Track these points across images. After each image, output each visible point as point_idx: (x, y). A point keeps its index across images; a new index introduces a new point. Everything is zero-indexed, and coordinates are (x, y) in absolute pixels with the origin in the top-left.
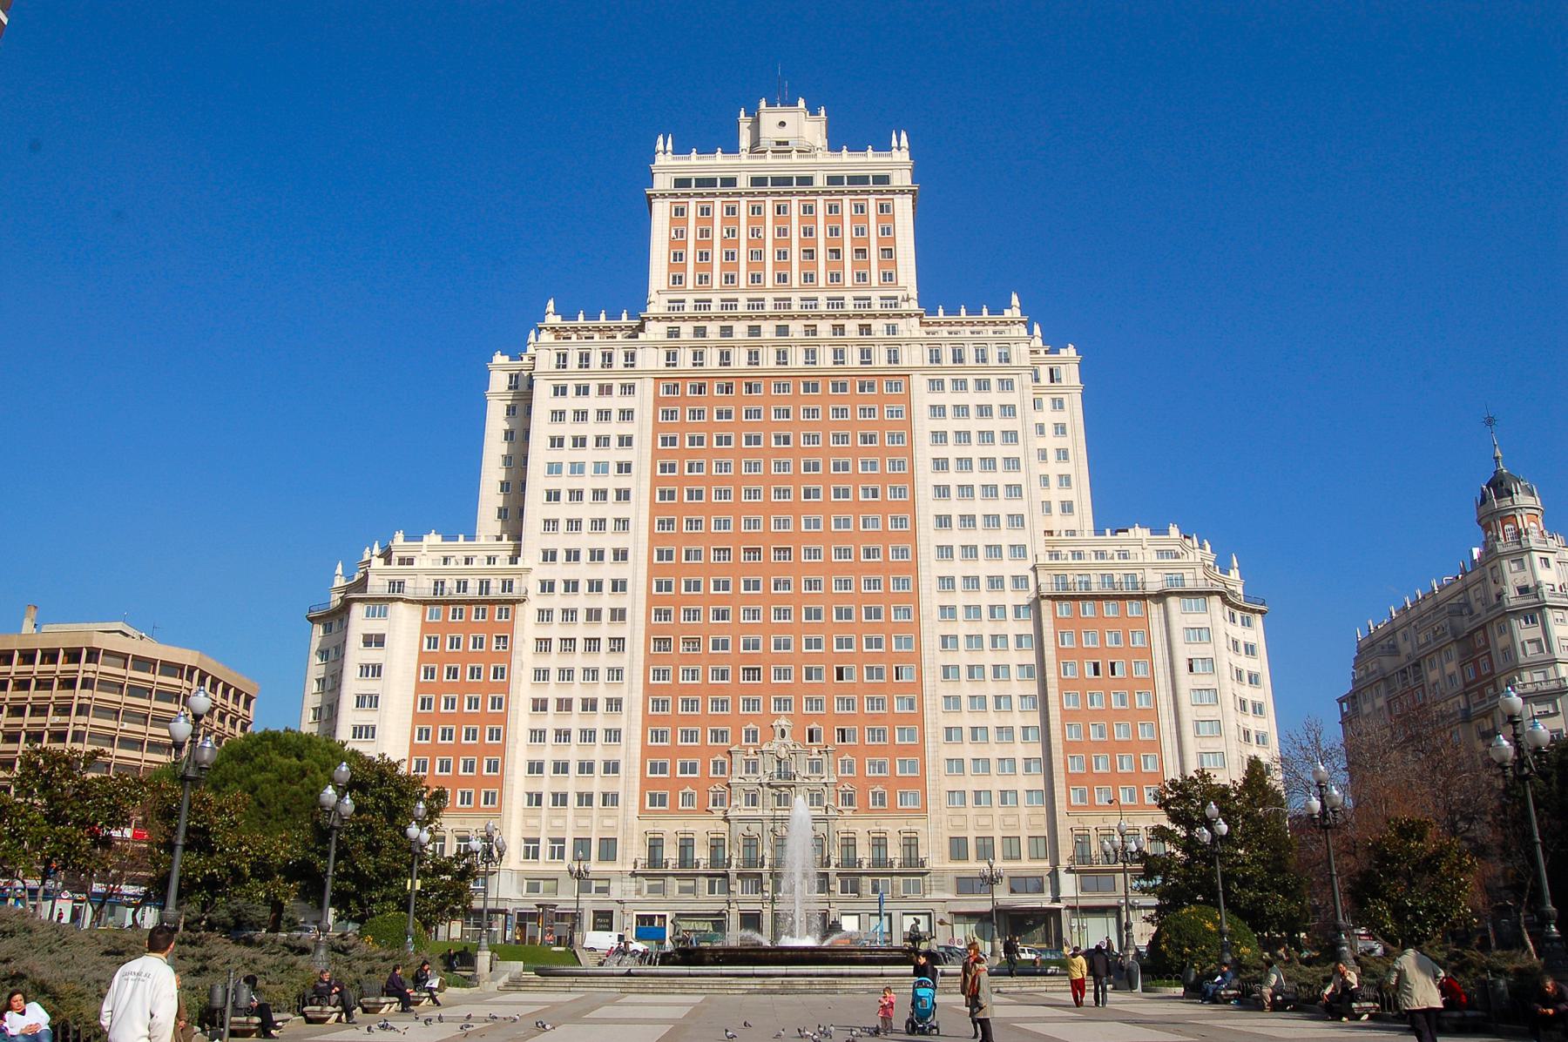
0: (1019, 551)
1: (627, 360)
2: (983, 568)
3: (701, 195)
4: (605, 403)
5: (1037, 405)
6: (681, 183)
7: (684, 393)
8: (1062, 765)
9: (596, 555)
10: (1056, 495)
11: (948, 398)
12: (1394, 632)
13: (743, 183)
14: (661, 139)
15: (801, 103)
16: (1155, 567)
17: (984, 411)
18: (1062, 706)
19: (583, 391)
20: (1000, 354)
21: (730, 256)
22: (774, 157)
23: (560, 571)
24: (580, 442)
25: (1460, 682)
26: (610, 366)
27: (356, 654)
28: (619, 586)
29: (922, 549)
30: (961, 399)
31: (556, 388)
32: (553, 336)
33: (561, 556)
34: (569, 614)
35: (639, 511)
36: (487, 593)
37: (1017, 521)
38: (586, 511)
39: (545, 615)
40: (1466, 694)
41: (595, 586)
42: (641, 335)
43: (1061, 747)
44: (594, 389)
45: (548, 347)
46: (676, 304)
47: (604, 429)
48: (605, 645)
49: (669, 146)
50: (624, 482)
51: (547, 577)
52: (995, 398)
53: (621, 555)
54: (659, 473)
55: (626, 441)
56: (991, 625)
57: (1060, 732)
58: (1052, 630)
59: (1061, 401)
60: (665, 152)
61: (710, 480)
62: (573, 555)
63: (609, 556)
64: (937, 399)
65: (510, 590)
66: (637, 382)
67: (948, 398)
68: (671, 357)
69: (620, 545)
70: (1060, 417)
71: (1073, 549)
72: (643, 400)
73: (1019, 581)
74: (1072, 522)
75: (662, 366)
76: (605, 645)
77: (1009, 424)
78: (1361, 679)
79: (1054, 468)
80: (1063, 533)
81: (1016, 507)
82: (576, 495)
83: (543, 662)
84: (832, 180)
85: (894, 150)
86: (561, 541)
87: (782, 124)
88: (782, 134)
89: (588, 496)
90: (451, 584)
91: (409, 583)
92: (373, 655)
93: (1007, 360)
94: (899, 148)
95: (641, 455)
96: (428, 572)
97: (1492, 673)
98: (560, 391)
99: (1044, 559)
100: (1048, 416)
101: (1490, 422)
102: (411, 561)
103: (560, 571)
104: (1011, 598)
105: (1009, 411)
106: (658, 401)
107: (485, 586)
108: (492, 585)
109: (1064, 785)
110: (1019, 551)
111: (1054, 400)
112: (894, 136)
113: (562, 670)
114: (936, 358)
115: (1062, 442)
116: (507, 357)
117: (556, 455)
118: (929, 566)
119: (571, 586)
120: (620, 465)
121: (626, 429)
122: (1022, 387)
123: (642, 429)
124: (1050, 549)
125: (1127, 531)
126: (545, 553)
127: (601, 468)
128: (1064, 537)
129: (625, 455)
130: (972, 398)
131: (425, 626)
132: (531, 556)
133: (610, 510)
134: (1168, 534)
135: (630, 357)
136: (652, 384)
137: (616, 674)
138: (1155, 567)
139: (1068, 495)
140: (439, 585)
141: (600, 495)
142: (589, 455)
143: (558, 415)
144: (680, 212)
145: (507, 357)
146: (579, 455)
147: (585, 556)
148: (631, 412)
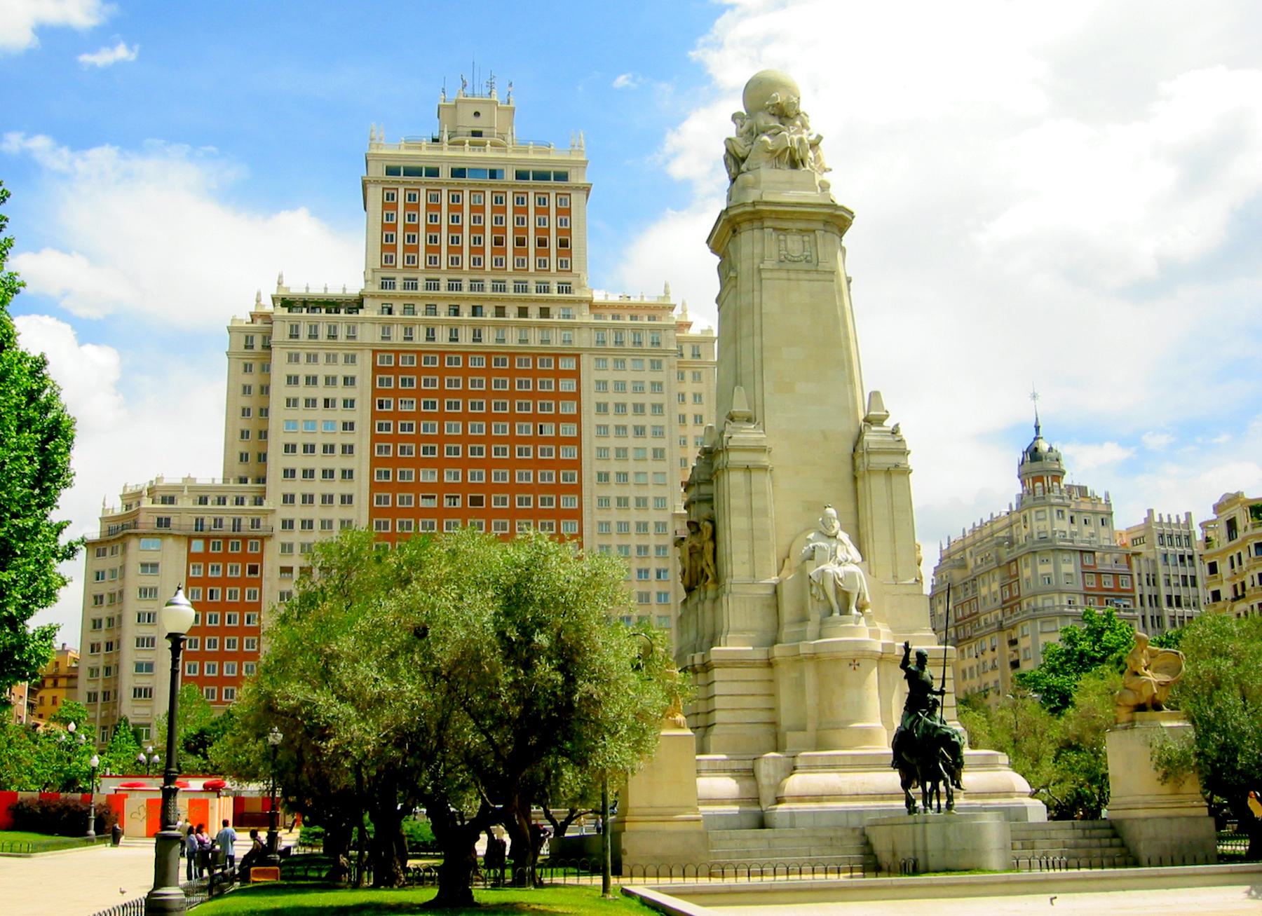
2: (633, 516)
3: (409, 183)
4: (331, 370)
5: (681, 377)
6: (392, 171)
7: (397, 363)
11: (611, 376)
12: (964, 549)
19: (312, 358)
20: (653, 338)
23: (298, 512)
24: (311, 403)
25: (999, 598)
26: (335, 337)
27: (135, 579)
29: (586, 500)
30: (620, 376)
31: (290, 355)
32: (286, 309)
33: (298, 499)
35: (361, 463)
36: (239, 530)
38: (318, 462)
39: (287, 548)
40: (1003, 609)
42: (360, 311)
47: (330, 393)
50: (348, 439)
51: (288, 516)
52: (648, 376)
53: (347, 500)
55: (348, 403)
59: (699, 374)
62: (308, 499)
64: (602, 376)
67: (611, 376)
69: (347, 492)
70: (697, 388)
72: (362, 370)
75: (378, 340)
77: (657, 399)
78: (936, 586)
82: (310, 449)
84: (521, 175)
86: (298, 487)
87: (477, 114)
90: (209, 521)
91: (174, 521)
92: (149, 581)
95: (362, 415)
96: (189, 511)
97: (1019, 596)
98: (294, 358)
100: (689, 387)
101: (1034, 396)
102: (172, 500)
103: (298, 512)
104: (652, 540)
105: (657, 386)
106: (376, 370)
107: (237, 525)
108: (242, 523)
111: (694, 373)
117: (292, 414)
118: (592, 512)
121: (349, 393)
122: (670, 367)
123: (362, 393)
126: (285, 497)
129: (348, 416)
130: (628, 376)
131: (192, 557)
132: (272, 501)
133: (337, 462)
140: (199, 523)
141: (329, 449)
142: (319, 413)
143: (292, 380)
144: (391, 197)
146: (312, 414)
147: (317, 500)
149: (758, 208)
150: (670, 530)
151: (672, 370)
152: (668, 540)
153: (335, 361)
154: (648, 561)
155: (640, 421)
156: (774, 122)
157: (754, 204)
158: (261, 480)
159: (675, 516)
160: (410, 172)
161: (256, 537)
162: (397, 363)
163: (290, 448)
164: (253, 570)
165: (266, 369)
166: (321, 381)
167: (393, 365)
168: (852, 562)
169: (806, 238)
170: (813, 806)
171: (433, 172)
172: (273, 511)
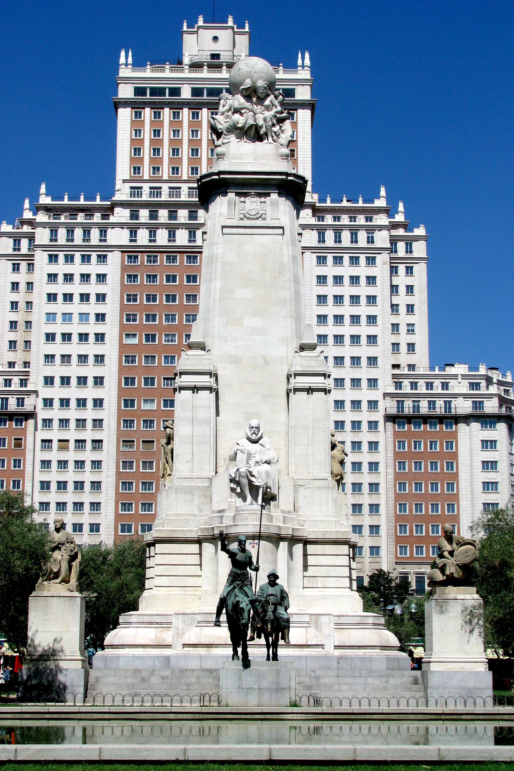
0: (373, 383)
1: (101, 236)
4: (86, 269)
7: (142, 262)
8: (394, 531)
9: (82, 381)
10: (404, 339)
13: (186, 93)
14: (123, 53)
15: (230, 23)
16: (466, 396)
17: (355, 280)
18: (395, 491)
20: (368, 237)
21: (175, 151)
22: (209, 72)
24: (68, 297)
26: (89, 240)
28: (98, 403)
31: (50, 256)
34: (64, 423)
36: (6, 408)
37: (372, 361)
41: (82, 403)
43: (394, 518)
44: (78, 256)
45: (43, 225)
46: (136, 190)
47: (85, 289)
48: (89, 445)
49: (130, 60)
50: (100, 329)
54: (125, 322)
55: (101, 298)
56: (352, 434)
57: (393, 508)
58: (392, 439)
59: (412, 268)
60: (126, 65)
61: (160, 328)
62: (65, 381)
63: (90, 381)
64: (322, 271)
65: (23, 405)
66: (110, 255)
68: (133, 233)
70: (409, 281)
71: (412, 380)
73: (373, 404)
74: (412, 359)
76: (89, 445)
79: (403, 319)
80: (406, 369)
81: (372, 351)
82: (67, 337)
83: (46, 456)
85: (300, 68)
87: (215, 39)
88: (215, 48)
89: (75, 338)
93: (373, 242)
94: (303, 66)
98: (53, 259)
99: (392, 390)
105: (371, 280)
106: (124, 268)
109: (394, 543)
110: (373, 383)
111: (407, 268)
112: (300, 56)
113: (59, 462)
114: (321, 239)
115: (410, 300)
116: (11, 226)
117: (52, 308)
119: (65, 403)
120: (97, 315)
122: (384, 263)
124: (396, 380)
125: (453, 365)
126: (46, 378)
127: (84, 317)
128: (406, 372)
129: (100, 309)
134: (478, 371)
135: (103, 233)
136: (120, 255)
137: (97, 464)
138: (466, 396)
139: (411, 339)
141: (83, 337)
143: (52, 277)
144: (138, 115)
145: (11, 226)
146: (68, 308)
147: (74, 381)
148: (104, 276)
149: (221, 176)
150: (381, 405)
151: (385, 266)
152: (379, 416)
153: (89, 261)
154: (360, 434)
155: (355, 311)
156: (248, 105)
157: (220, 173)
158: (26, 364)
159: (385, 395)
160: (155, 92)
161: (21, 414)
162: (142, 262)
163: (50, 337)
164: (19, 443)
165: (31, 267)
166: (77, 278)
167: (139, 263)
168: (268, 463)
169: (263, 199)
170: (202, 651)
171: (175, 92)
172: (36, 392)
